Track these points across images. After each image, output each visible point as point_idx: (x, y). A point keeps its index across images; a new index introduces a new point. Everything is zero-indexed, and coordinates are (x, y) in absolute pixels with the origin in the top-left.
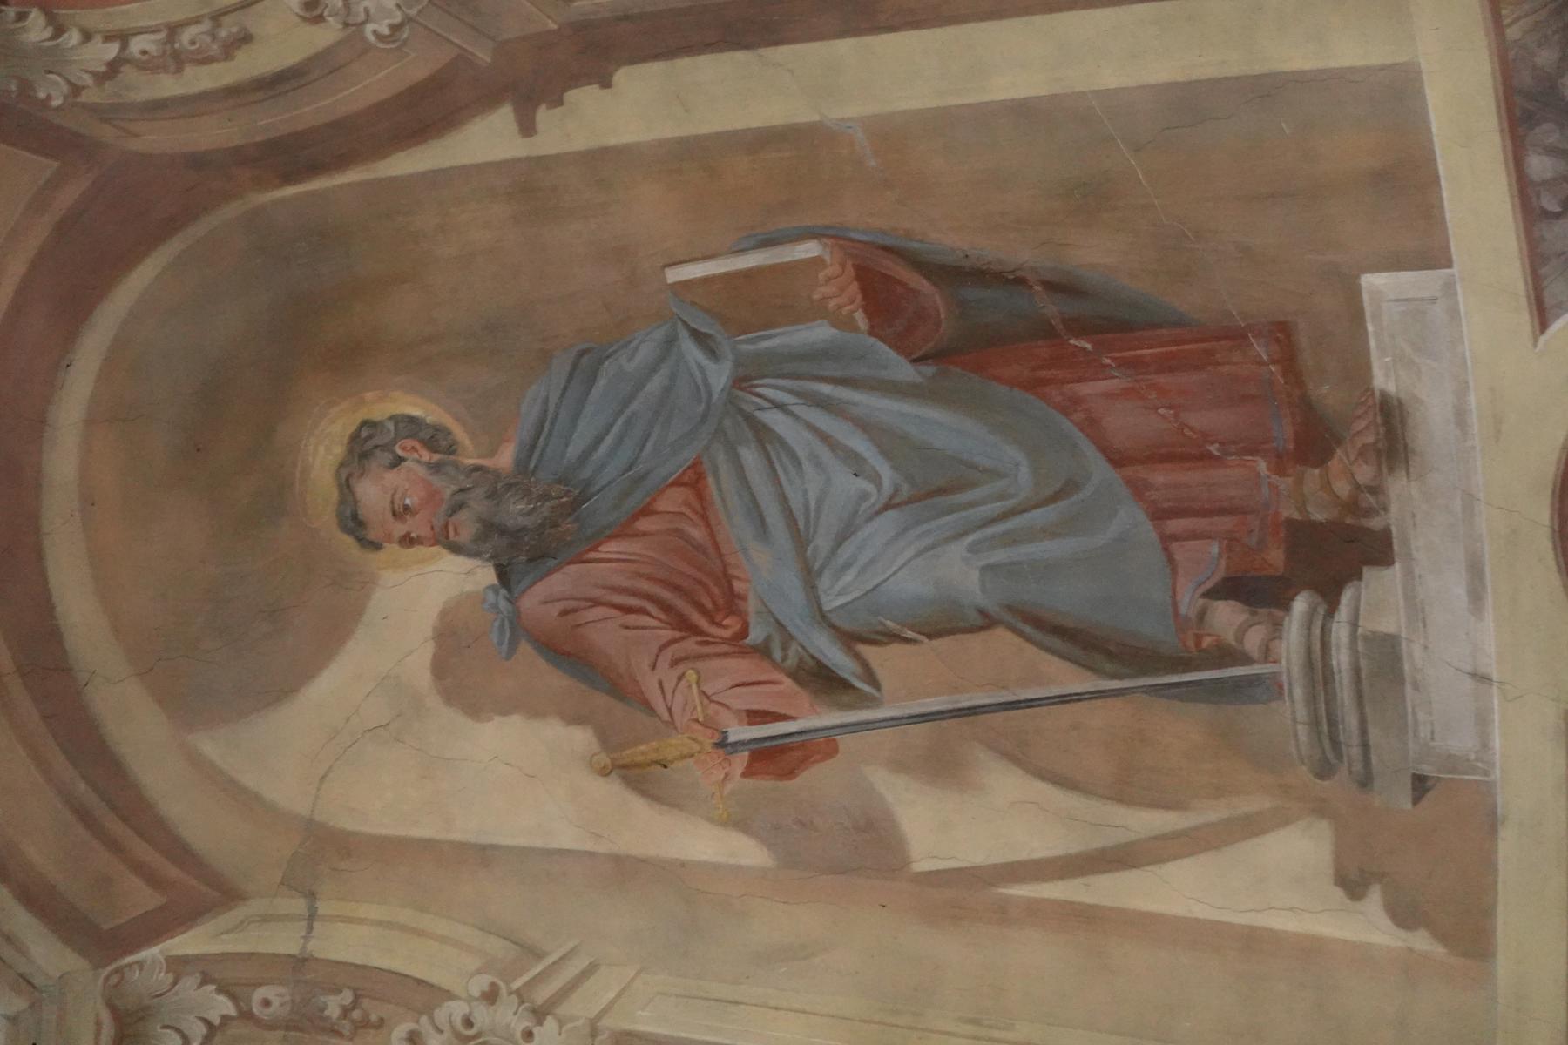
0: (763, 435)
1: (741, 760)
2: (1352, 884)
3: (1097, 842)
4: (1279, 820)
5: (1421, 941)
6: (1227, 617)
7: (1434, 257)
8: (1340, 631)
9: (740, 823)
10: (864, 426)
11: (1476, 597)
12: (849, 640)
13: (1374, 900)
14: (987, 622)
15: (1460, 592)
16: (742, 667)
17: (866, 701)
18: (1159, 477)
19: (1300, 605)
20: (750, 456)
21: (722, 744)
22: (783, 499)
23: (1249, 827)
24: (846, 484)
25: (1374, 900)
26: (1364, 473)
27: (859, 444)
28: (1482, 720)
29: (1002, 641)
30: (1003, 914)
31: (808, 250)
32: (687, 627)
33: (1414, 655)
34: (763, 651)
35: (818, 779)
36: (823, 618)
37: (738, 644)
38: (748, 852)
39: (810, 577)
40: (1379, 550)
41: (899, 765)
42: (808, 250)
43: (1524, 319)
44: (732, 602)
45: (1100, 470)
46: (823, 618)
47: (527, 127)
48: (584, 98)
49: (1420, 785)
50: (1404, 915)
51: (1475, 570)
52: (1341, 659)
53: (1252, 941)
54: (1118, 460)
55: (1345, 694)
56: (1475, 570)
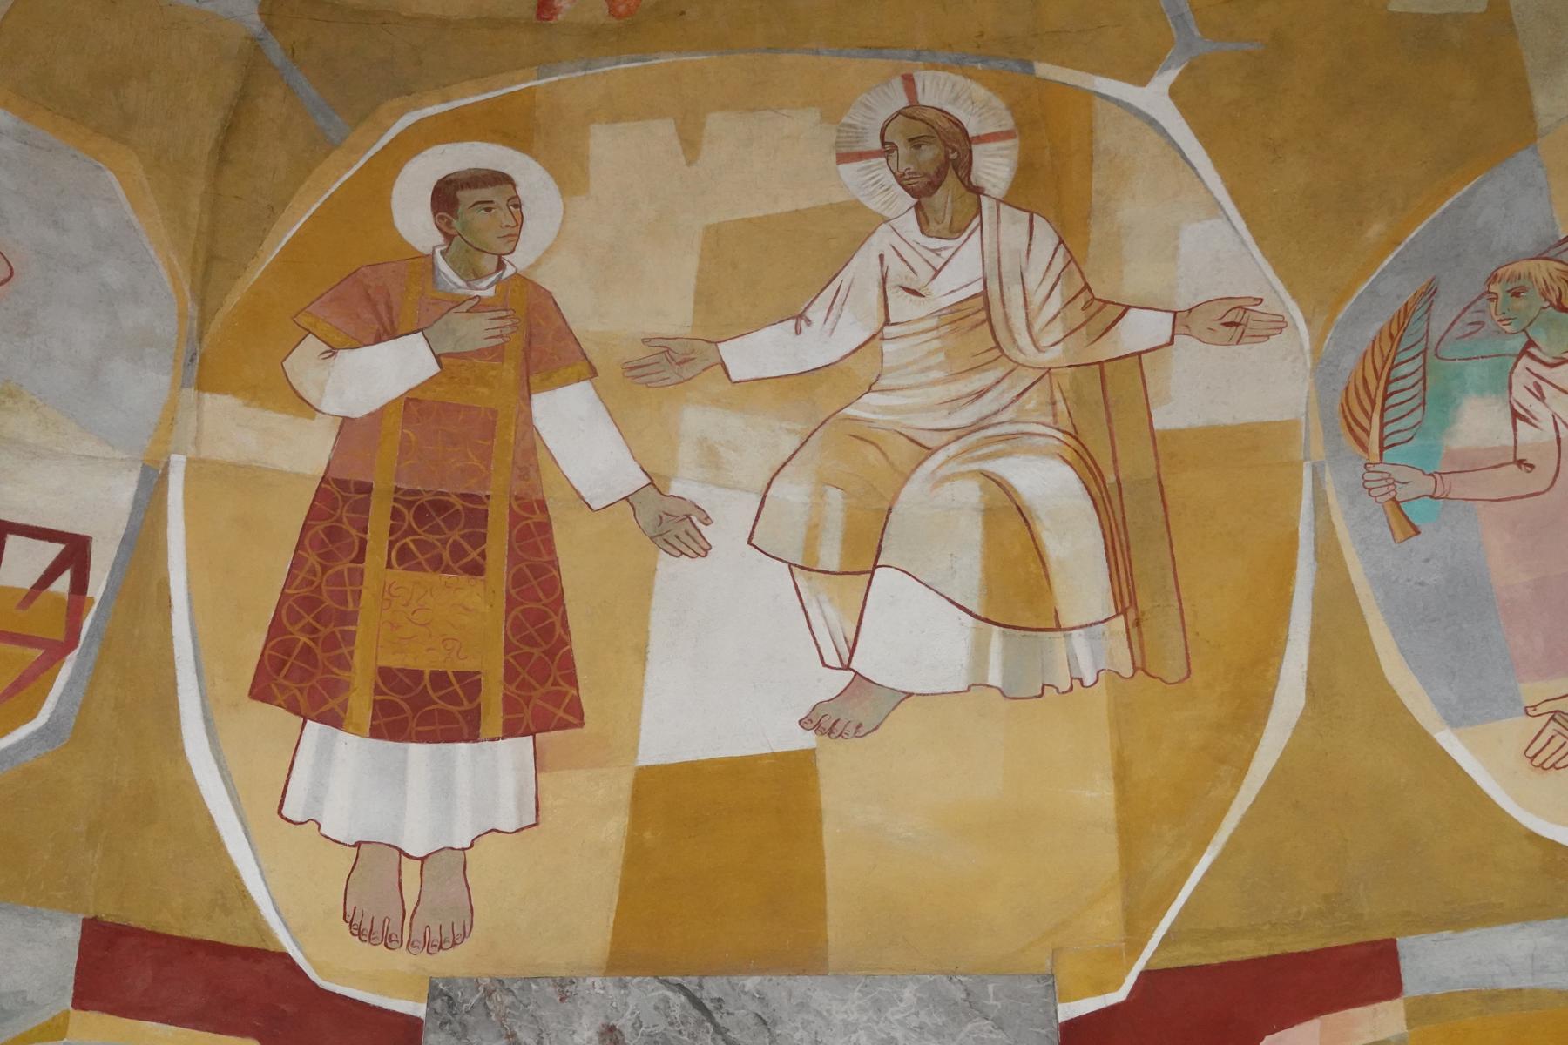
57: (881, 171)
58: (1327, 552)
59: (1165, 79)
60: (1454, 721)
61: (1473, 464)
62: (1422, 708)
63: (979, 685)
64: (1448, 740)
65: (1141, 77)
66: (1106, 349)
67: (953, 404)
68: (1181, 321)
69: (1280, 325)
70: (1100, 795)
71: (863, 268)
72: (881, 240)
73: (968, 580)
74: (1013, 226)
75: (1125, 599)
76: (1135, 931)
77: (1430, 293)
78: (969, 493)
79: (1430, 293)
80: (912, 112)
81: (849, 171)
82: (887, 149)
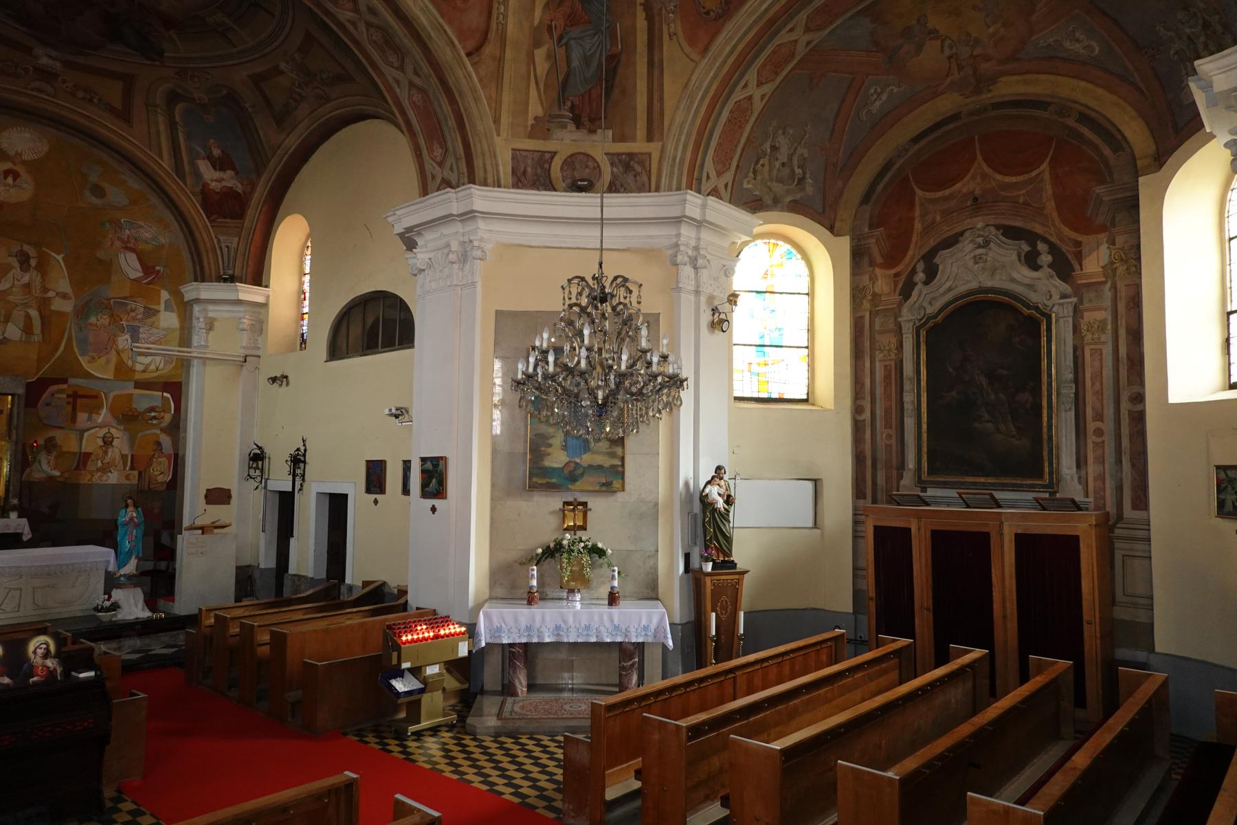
0: (595, 34)
1: (549, 23)
2: (536, 118)
3: (539, 80)
4: (543, 108)
5: (529, 129)
6: (569, 104)
7: (614, 141)
8: (567, 120)
9: (540, 22)
10: (595, 52)
11: (572, 140)
12: (566, 44)
13: (533, 122)
14: (569, 66)
15: (574, 138)
16: (563, 25)
17: (558, 45)
18: (587, 97)
19: (571, 115)
20: (592, 32)
21: (552, 21)
22: (586, 36)
23: (542, 104)
24: (588, 47)
25: (533, 122)
26: (587, 126)
27: (593, 50)
28: (557, 140)
29: (566, 70)
30: (529, 65)
31: (620, 47)
32: (569, 16)
33: (565, 131)
34: (565, 29)
35: (546, 36)
36: (569, 40)
37: (566, 25)
38: (536, 22)
39: (575, 39)
40: (578, 128)
41: (548, 49)
42: (620, 47)
43: (607, 152)
44: (572, 25)
45: (588, 88)
46: (569, 40)
47: (641, 4)
48: (644, 14)
49: (548, 130)
50: (532, 125)
51: (575, 141)
52: (564, 120)
53: (527, 103)
54: (590, 90)
55: (560, 120)
56: (575, 141)
57: (15, 259)
58: (70, 328)
59: (62, 256)
60: (80, 355)
61: (91, 324)
62: (78, 354)
63: (21, 340)
64: (80, 358)
65: (58, 254)
66: (46, 296)
67: (22, 300)
68: (57, 294)
69: (70, 298)
70: (35, 357)
71: (10, 275)
72: (14, 271)
73: (21, 325)
74: (35, 273)
75: (42, 333)
76: (37, 374)
77: (91, 300)
78: (22, 313)
79: (91, 300)
80: (22, 251)
81: (10, 258)
82: (16, 256)
